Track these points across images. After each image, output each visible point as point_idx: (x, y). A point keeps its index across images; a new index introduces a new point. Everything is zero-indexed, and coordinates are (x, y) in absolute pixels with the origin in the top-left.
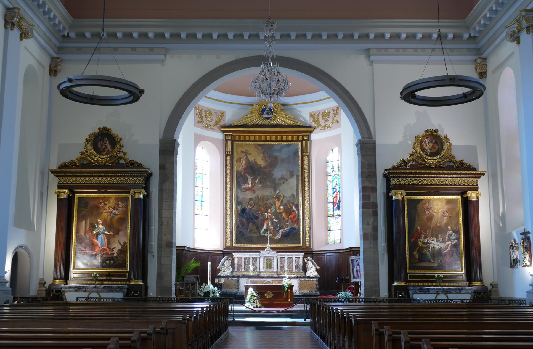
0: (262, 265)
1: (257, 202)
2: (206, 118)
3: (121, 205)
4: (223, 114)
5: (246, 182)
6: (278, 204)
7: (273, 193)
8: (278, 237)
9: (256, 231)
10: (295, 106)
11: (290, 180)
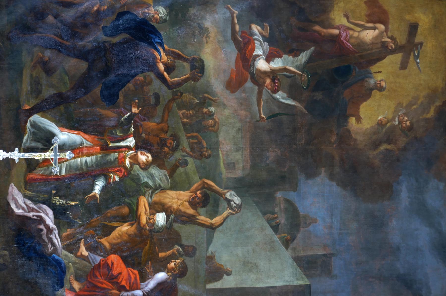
1: (187, 97)
6: (178, 199)
7: (225, 173)
9: (48, 92)
11: (287, 255)
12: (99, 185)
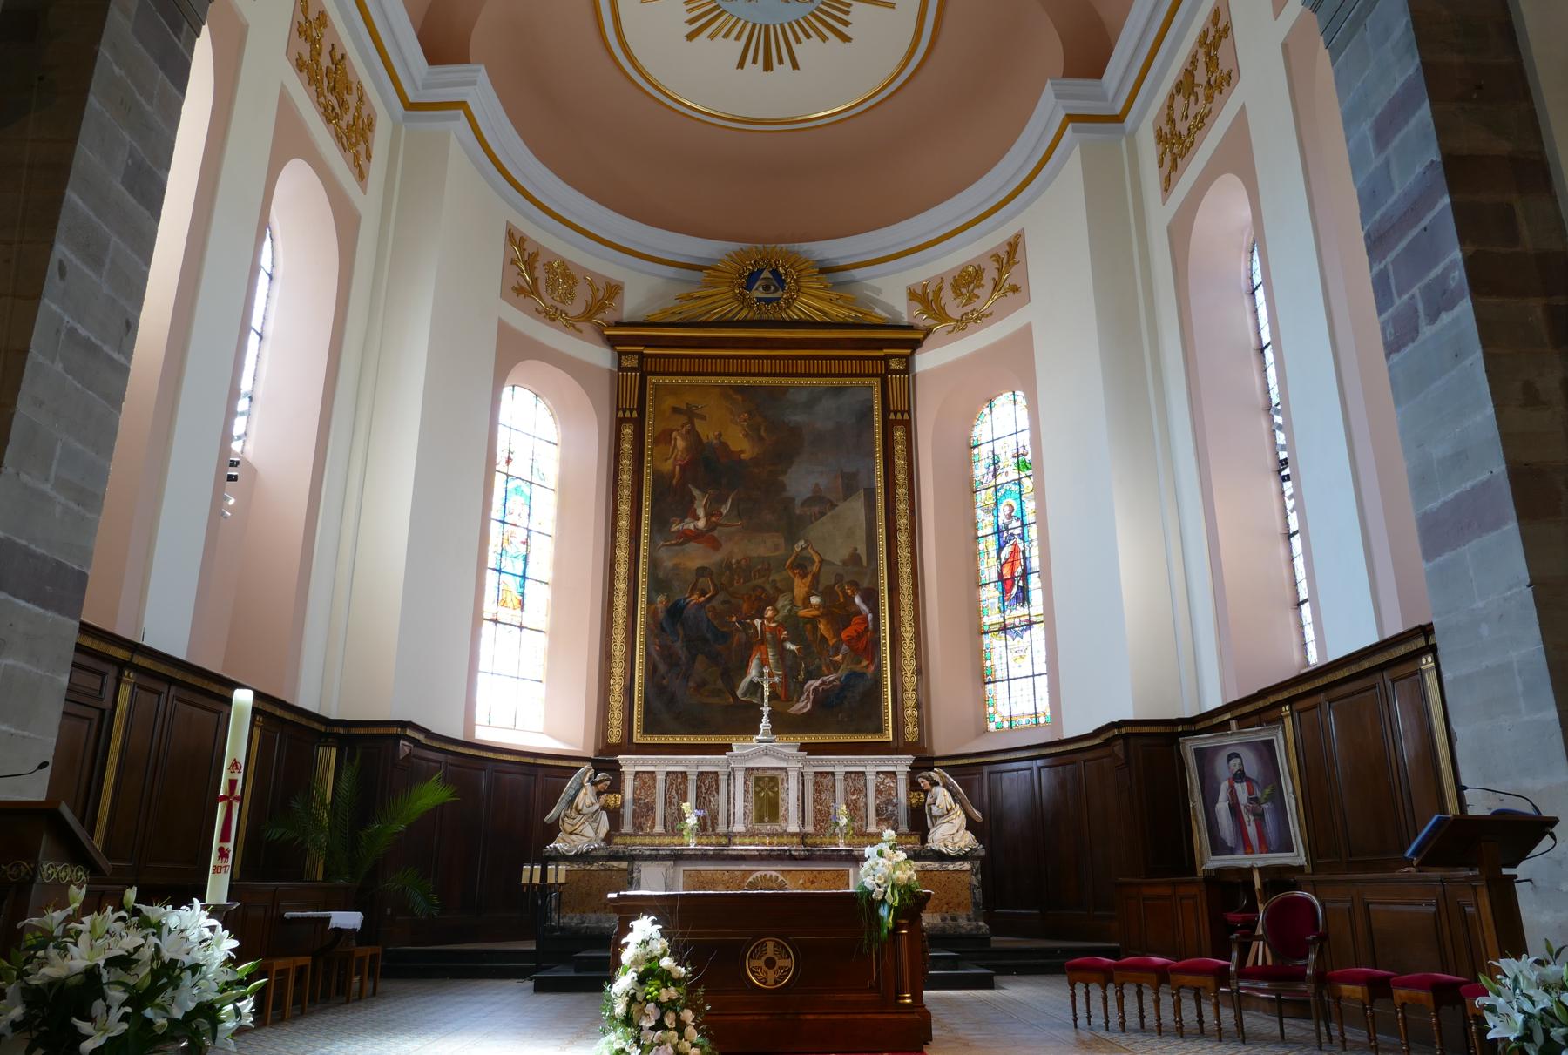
0: (739, 803)
1: (724, 580)
2: (552, 284)
4: (614, 290)
6: (800, 588)
7: (781, 552)
8: (803, 706)
9: (720, 684)
10: (857, 274)
11: (842, 506)
12: (790, 646)
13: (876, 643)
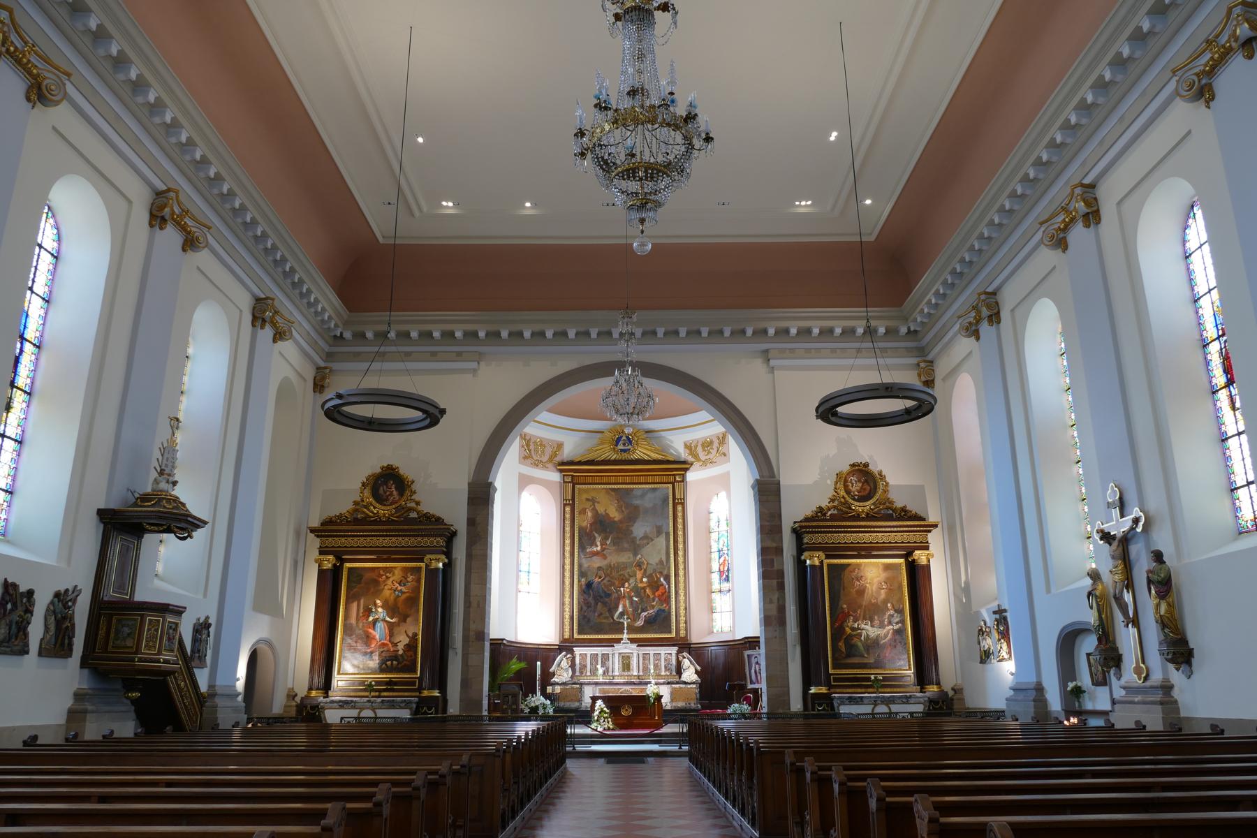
2: (536, 451)
3: (410, 578)
4: (560, 446)
5: (593, 544)
8: (640, 623)
11: (656, 540)
13: (669, 597)
